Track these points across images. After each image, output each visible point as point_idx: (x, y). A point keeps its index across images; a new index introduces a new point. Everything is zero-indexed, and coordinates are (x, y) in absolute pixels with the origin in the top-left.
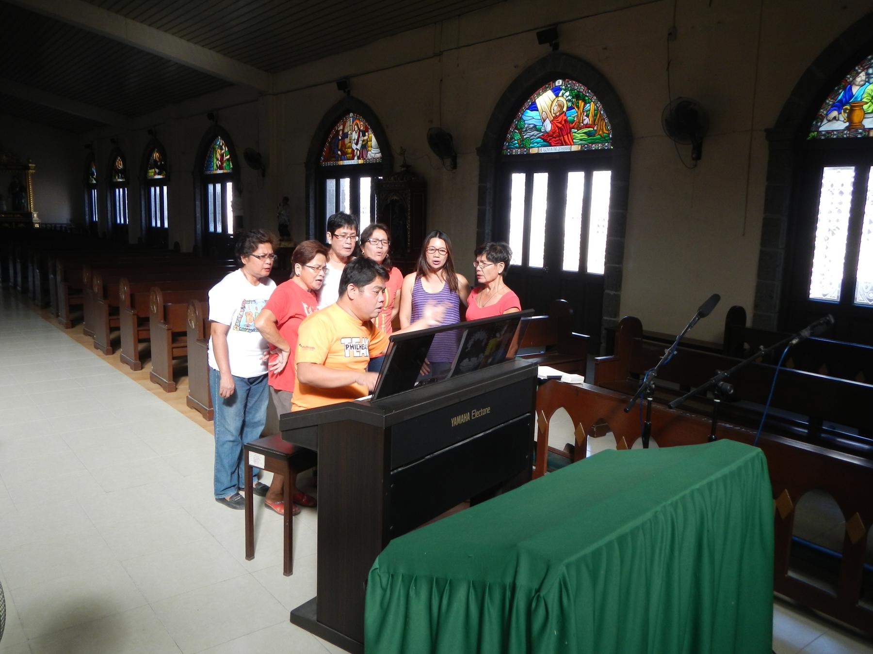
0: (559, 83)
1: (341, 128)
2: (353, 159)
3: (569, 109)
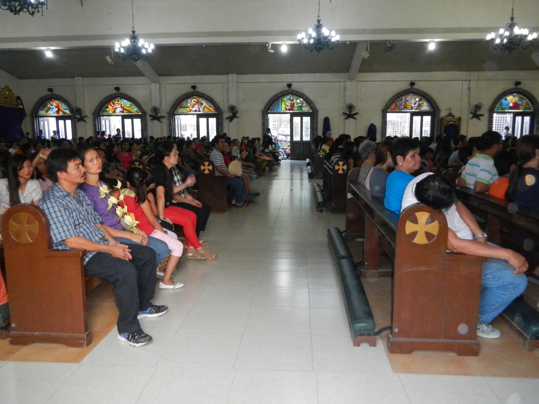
0: (515, 94)
1: (404, 98)
2: (412, 109)
3: (519, 101)
